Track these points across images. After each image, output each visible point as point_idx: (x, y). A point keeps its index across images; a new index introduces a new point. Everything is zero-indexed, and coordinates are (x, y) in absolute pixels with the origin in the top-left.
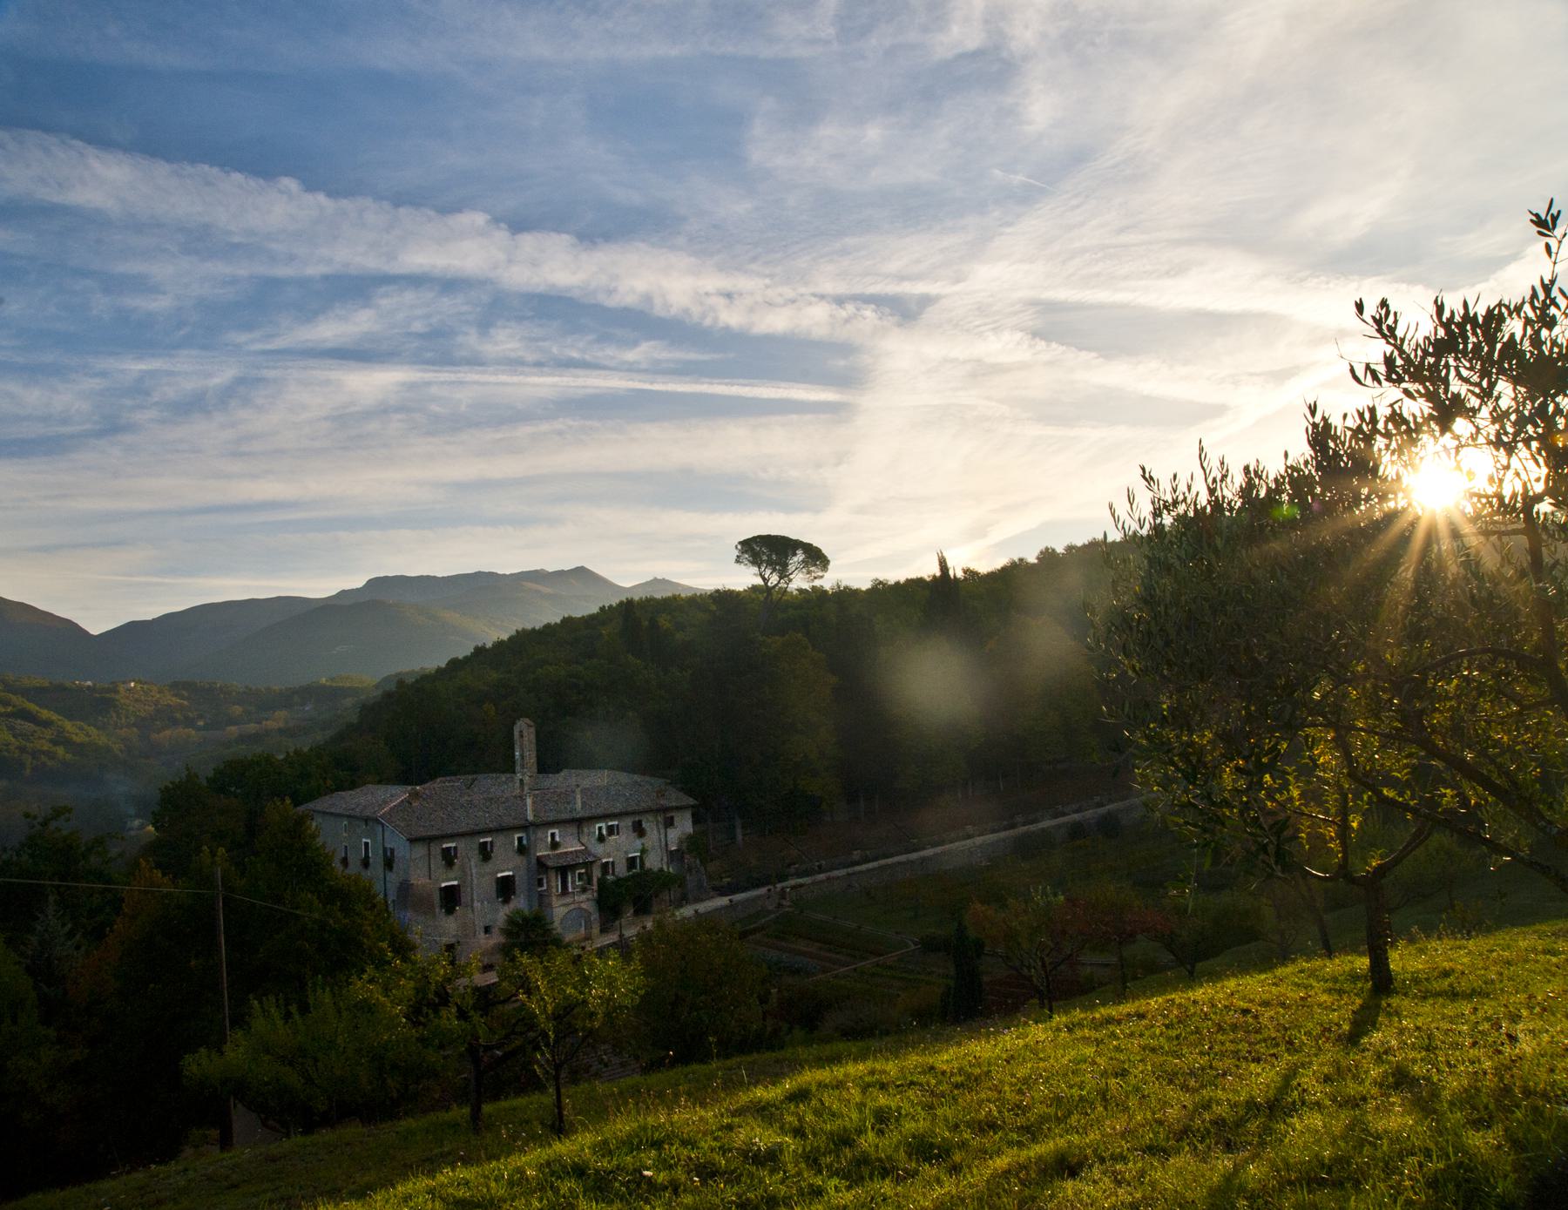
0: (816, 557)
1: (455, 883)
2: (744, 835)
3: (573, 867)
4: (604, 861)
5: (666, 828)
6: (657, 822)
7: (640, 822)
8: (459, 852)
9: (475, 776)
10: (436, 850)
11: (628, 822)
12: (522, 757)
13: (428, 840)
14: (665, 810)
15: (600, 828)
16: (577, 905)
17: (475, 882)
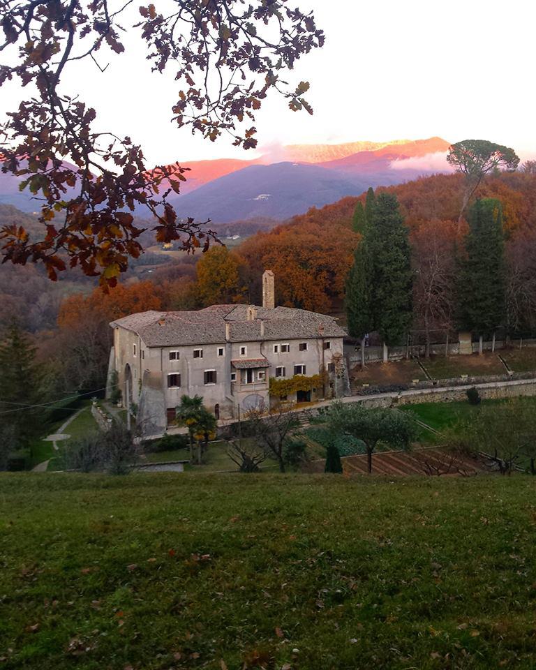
1: (178, 373)
2: (388, 357)
3: (256, 369)
5: (324, 349)
6: (318, 345)
7: (305, 345)
8: (180, 356)
9: (236, 305)
10: (166, 353)
11: (295, 345)
12: (266, 294)
13: (162, 347)
14: (323, 338)
15: (276, 347)
16: (254, 393)
17: (190, 373)
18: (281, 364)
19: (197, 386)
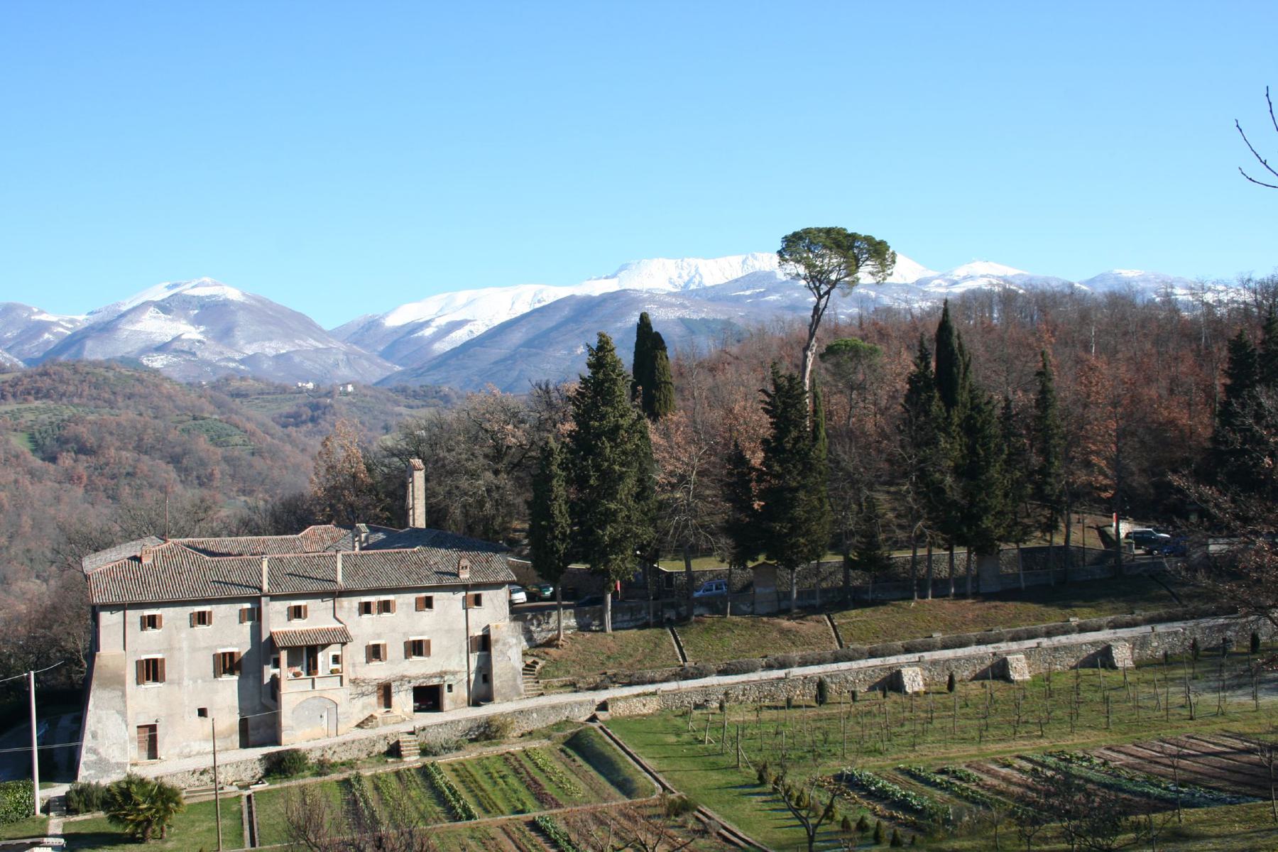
0: (878, 251)
4: (373, 642)
10: (134, 616)
14: (466, 588)
18: (379, 636)
19: (200, 681)
